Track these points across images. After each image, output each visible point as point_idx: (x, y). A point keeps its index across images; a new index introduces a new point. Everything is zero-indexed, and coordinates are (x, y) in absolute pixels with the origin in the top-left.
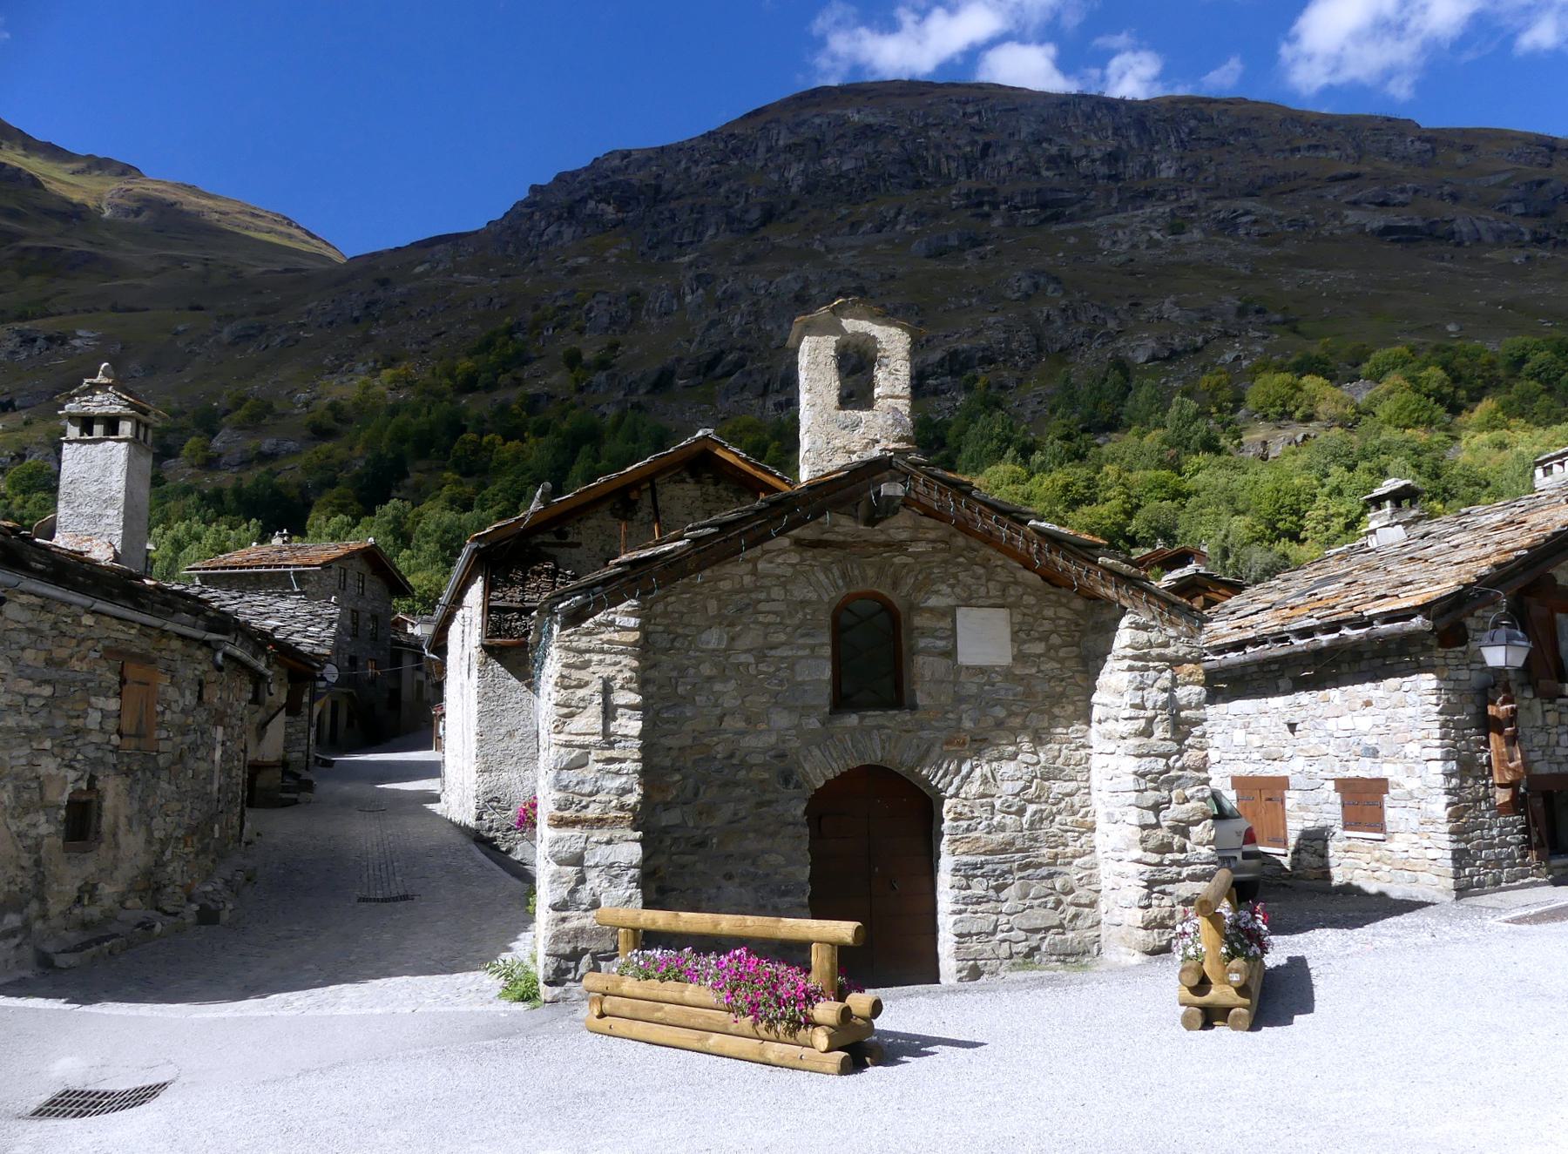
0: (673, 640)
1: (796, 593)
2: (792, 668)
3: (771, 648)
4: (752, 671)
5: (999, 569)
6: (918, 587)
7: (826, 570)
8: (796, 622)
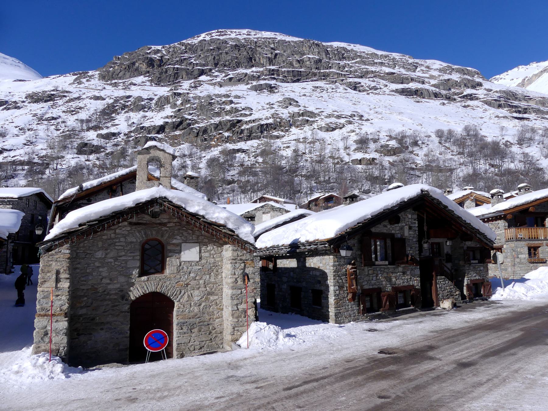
0: (86, 255)
1: (129, 240)
2: (126, 263)
3: (120, 257)
4: (113, 264)
5: (197, 231)
6: (169, 237)
7: (139, 232)
8: (128, 248)
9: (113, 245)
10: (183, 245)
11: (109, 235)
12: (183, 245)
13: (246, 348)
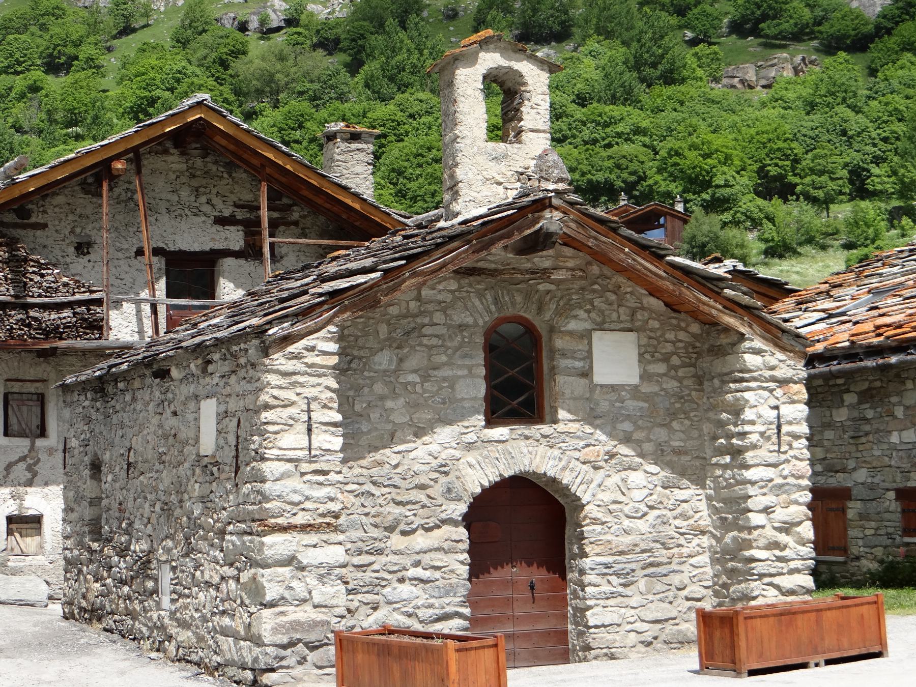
0: (350, 362)
1: (455, 318)
2: (452, 387)
3: (434, 369)
4: (418, 389)
5: (628, 296)
6: (559, 313)
7: (481, 295)
8: (455, 343)
9: (416, 334)
10: (596, 335)
11: (404, 305)
12: (596, 335)
13: (878, 608)
